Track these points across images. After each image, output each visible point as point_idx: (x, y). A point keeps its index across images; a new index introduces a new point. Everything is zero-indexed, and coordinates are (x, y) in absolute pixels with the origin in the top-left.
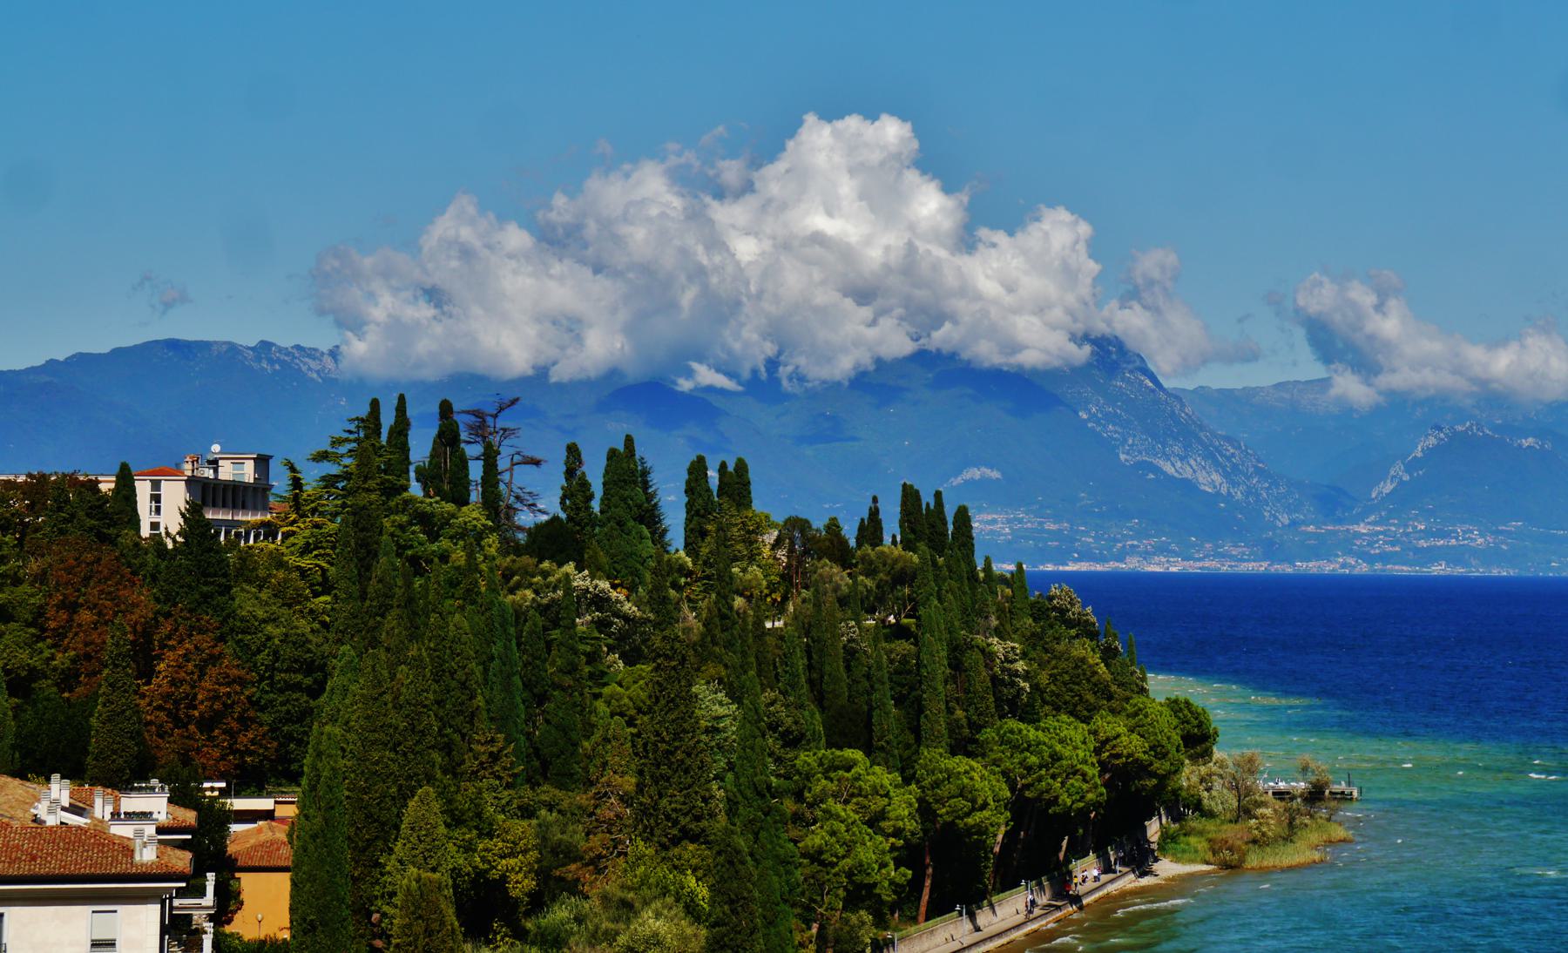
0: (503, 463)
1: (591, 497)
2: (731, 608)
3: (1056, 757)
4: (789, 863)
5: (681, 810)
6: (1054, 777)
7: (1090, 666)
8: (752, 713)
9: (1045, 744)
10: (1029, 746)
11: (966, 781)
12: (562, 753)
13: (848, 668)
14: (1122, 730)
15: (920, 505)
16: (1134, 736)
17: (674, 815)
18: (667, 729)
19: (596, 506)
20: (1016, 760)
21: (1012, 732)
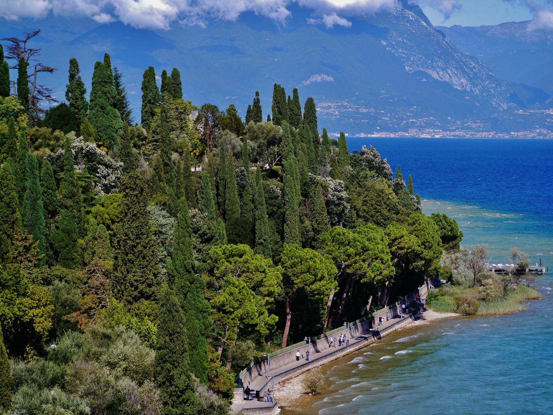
0: (30, 71)
1: (84, 92)
2: (170, 159)
3: (365, 249)
4: (205, 312)
5: (140, 280)
6: (364, 261)
7: (387, 195)
8: (184, 222)
9: (359, 241)
10: (349, 242)
11: (311, 263)
12: (67, 246)
13: (241, 196)
14: (405, 232)
15: (285, 97)
16: (413, 236)
17: (135, 284)
18: (132, 232)
19: (87, 97)
20: (342, 251)
21: (339, 234)
